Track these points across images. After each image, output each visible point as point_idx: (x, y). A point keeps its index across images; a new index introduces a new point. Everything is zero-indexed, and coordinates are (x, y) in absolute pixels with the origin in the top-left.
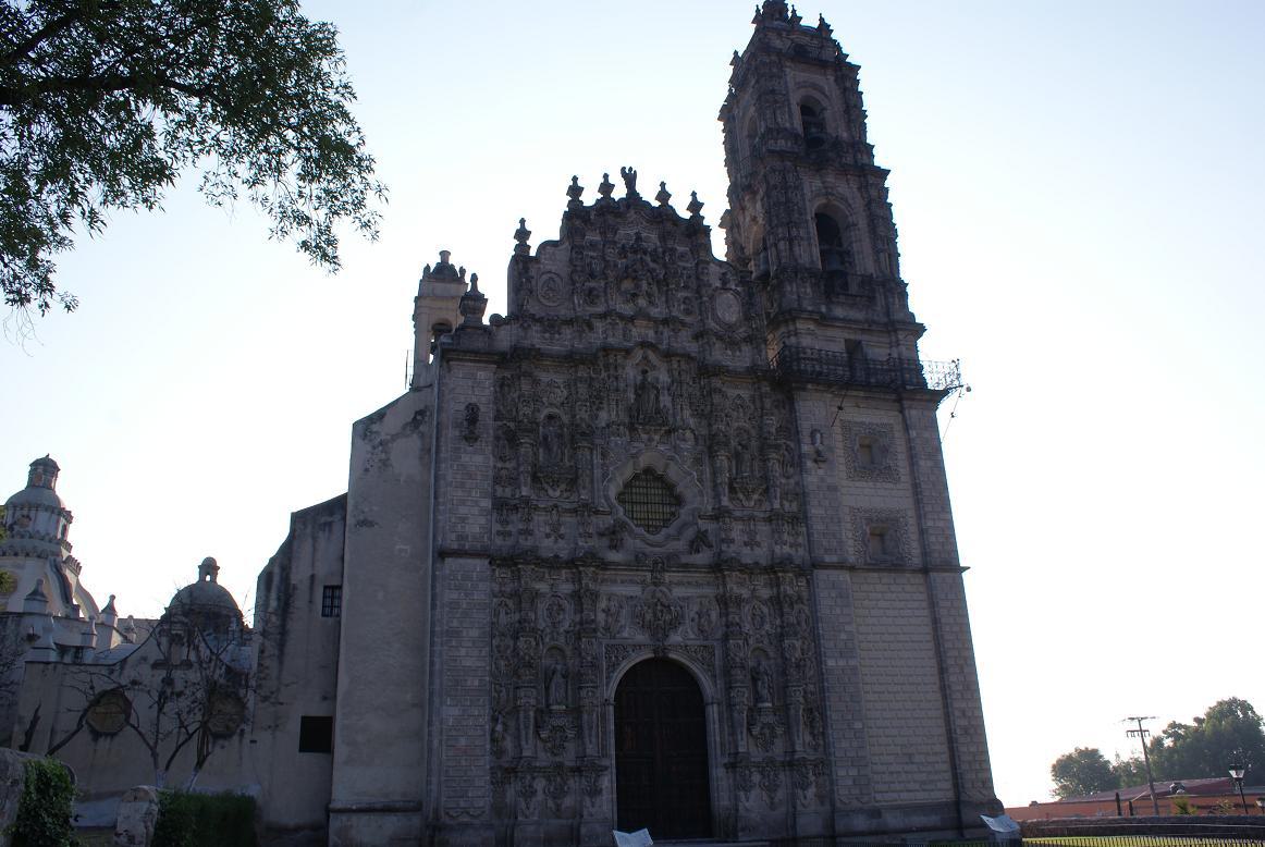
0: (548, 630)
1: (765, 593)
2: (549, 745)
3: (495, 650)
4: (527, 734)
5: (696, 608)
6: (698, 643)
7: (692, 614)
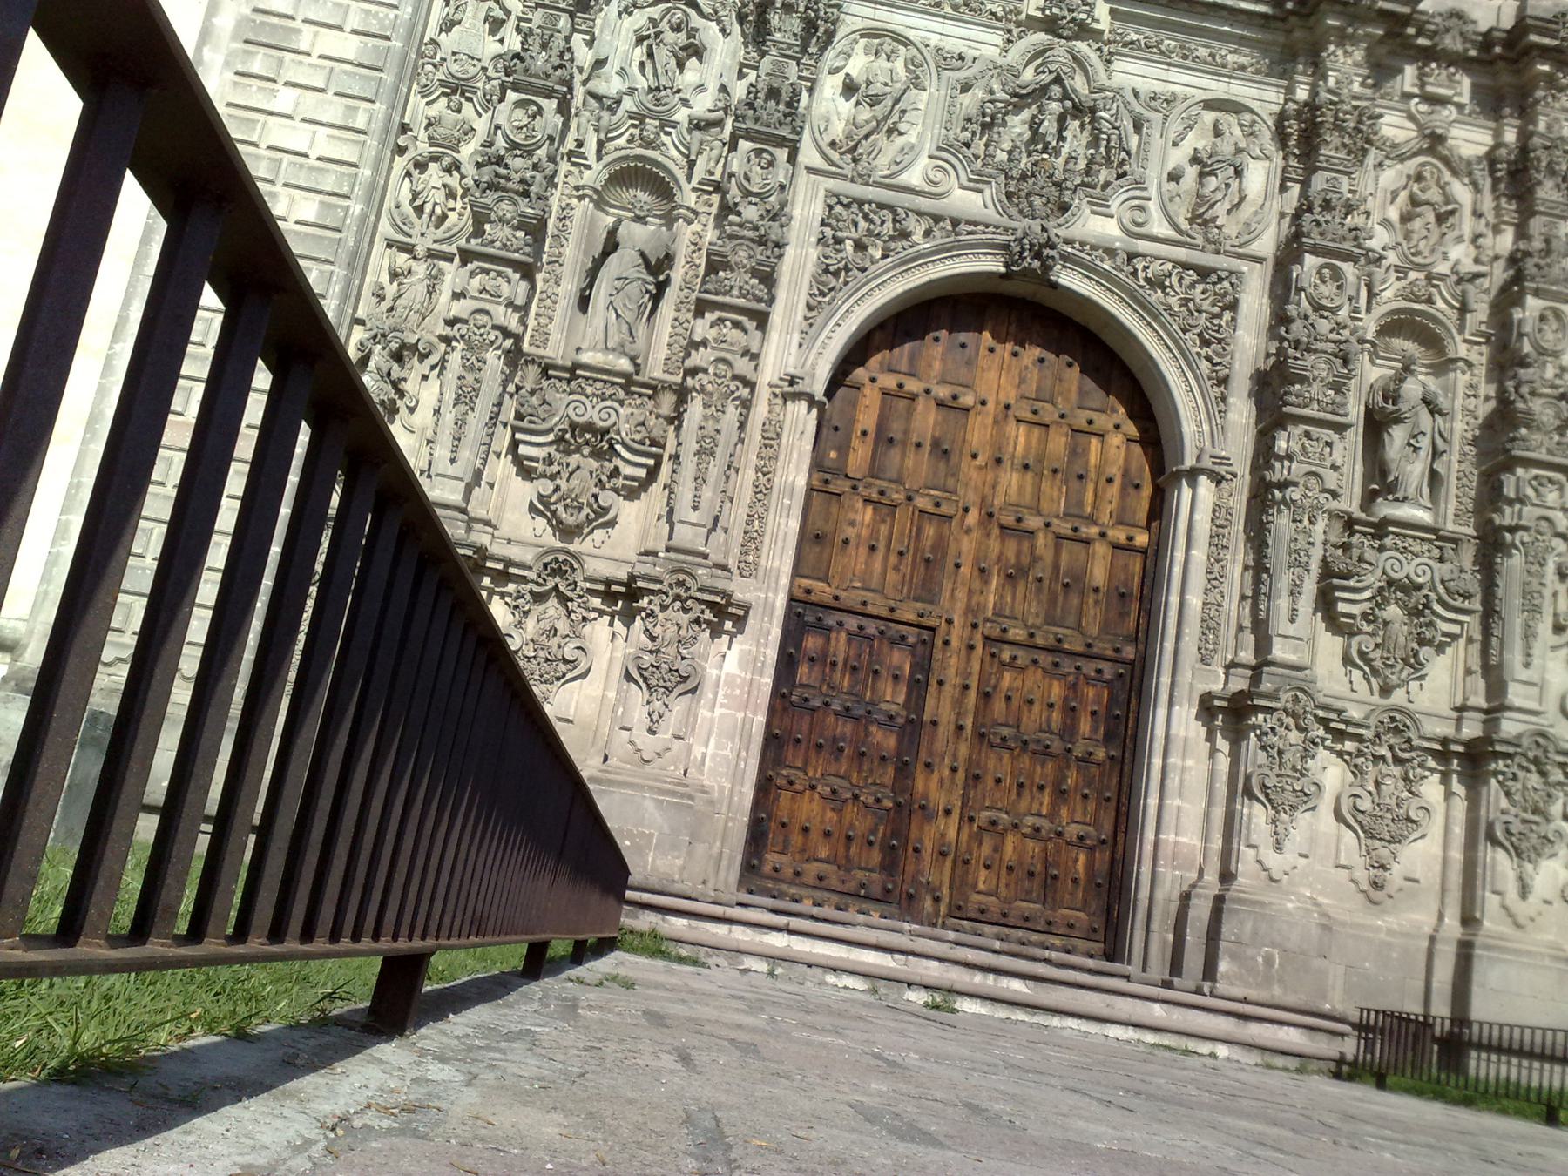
0: (628, 104)
1: (1470, 140)
2: (546, 486)
3: (423, 135)
4: (460, 423)
5: (1196, 141)
6: (1181, 253)
7: (1178, 157)
